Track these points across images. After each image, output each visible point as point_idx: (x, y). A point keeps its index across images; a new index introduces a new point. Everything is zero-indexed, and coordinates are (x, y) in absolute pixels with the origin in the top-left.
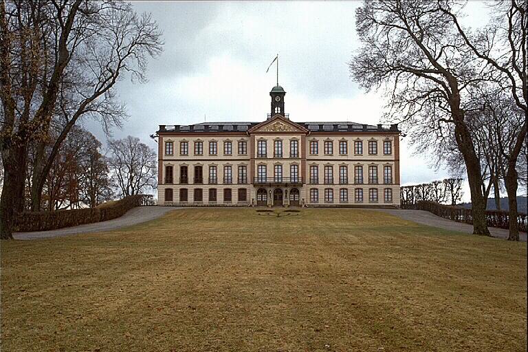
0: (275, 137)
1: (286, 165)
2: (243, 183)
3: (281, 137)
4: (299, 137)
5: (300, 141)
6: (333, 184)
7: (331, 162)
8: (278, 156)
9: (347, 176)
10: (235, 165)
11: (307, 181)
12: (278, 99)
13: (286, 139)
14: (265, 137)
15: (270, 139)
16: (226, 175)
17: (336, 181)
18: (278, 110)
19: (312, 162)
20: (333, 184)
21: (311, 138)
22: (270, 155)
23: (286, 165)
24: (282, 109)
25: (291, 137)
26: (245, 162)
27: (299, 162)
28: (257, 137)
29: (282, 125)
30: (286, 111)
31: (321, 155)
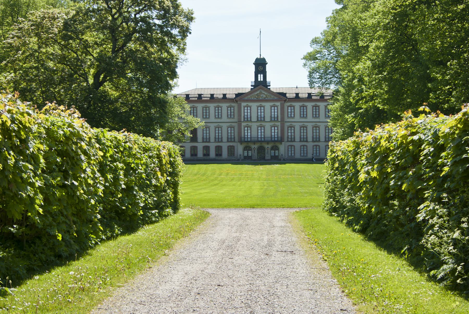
0: (258, 104)
1: (268, 126)
2: (231, 141)
3: (263, 104)
4: (278, 104)
5: (279, 107)
6: (307, 141)
7: (306, 124)
8: (261, 119)
9: (319, 135)
10: (225, 126)
11: (286, 139)
12: (261, 68)
13: (268, 105)
14: (250, 104)
15: (254, 105)
16: (217, 134)
17: (310, 139)
18: (260, 78)
19: (289, 124)
20: (307, 141)
21: (289, 104)
22: (254, 119)
23: (268, 126)
24: (265, 77)
25: (272, 104)
26: (233, 124)
27: (279, 124)
28: (243, 104)
29: (264, 94)
30: (268, 80)
31: (297, 118)
